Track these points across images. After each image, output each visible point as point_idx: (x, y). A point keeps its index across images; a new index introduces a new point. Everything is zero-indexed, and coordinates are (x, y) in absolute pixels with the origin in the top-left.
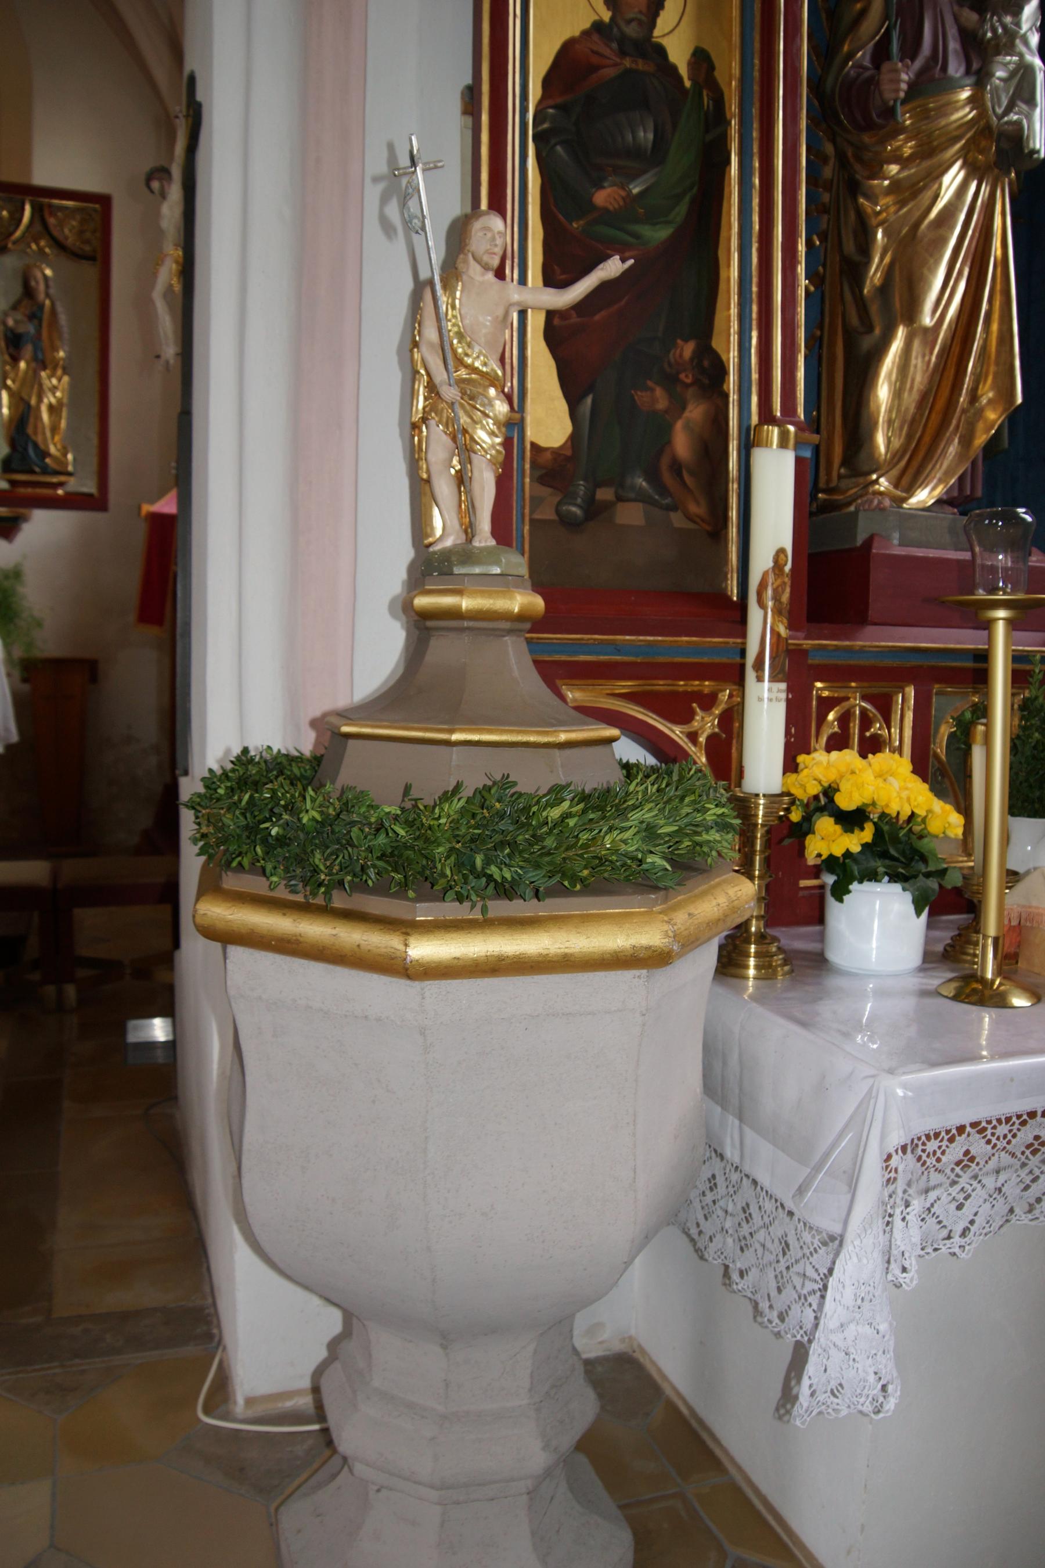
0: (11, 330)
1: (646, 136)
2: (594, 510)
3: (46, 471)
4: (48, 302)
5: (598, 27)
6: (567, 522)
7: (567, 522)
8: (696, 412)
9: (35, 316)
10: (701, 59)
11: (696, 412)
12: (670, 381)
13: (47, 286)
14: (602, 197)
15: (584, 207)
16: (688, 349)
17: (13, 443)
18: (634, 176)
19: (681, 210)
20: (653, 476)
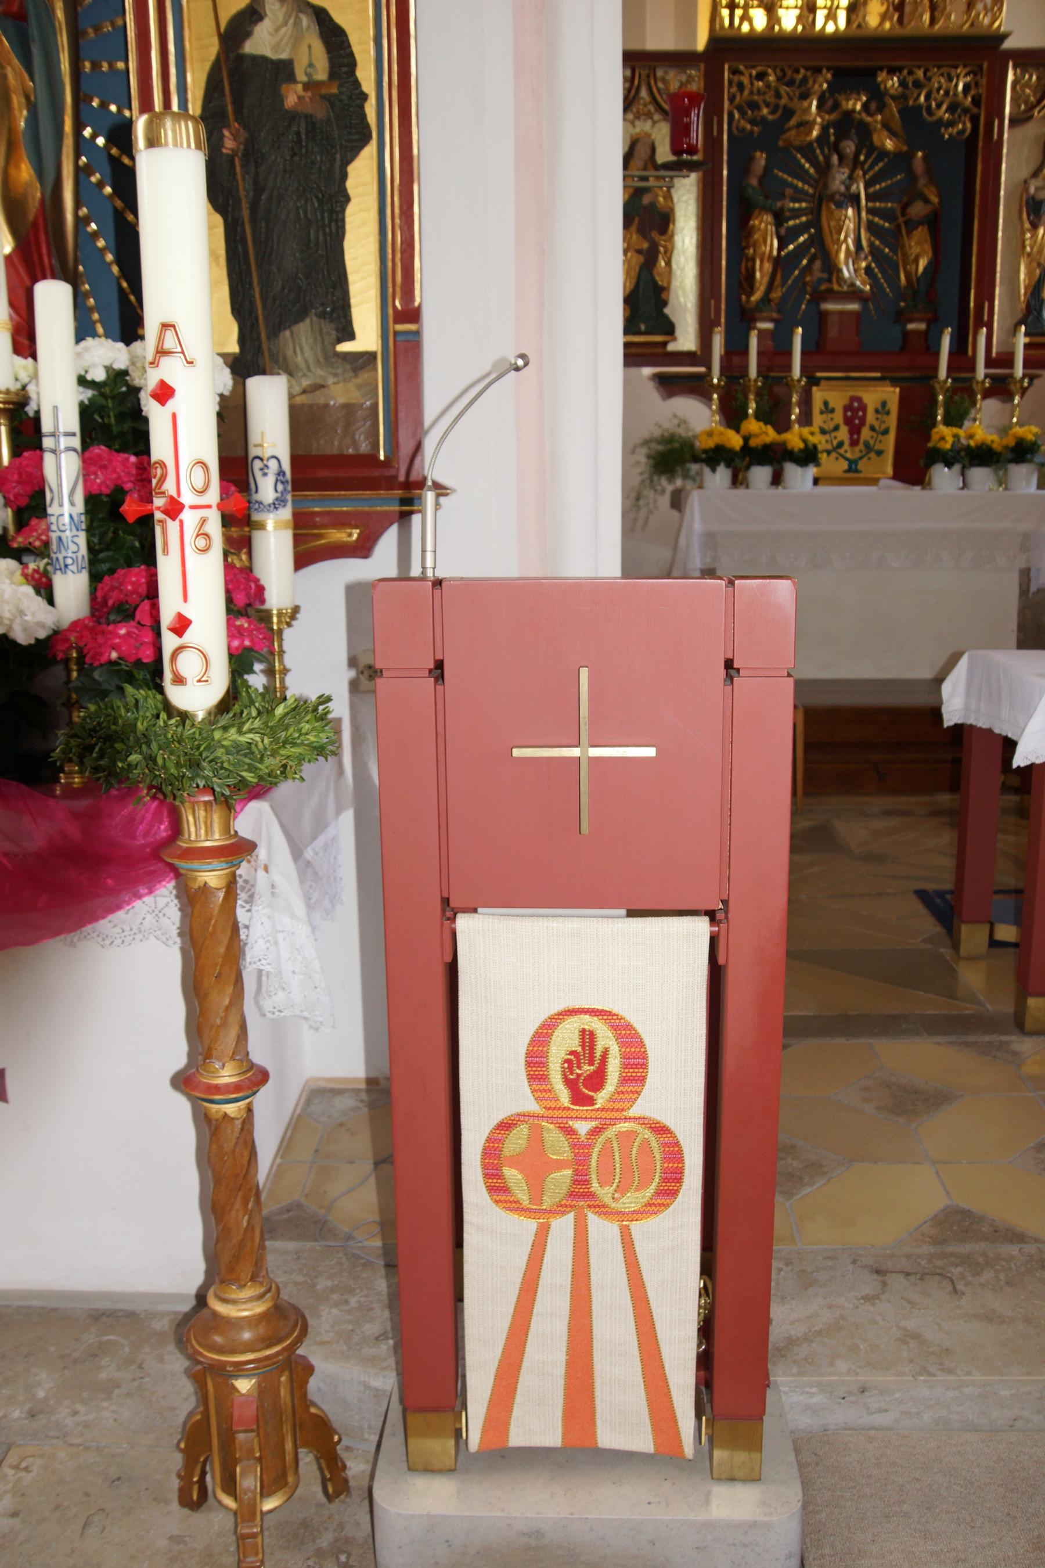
0: (1033, 198)
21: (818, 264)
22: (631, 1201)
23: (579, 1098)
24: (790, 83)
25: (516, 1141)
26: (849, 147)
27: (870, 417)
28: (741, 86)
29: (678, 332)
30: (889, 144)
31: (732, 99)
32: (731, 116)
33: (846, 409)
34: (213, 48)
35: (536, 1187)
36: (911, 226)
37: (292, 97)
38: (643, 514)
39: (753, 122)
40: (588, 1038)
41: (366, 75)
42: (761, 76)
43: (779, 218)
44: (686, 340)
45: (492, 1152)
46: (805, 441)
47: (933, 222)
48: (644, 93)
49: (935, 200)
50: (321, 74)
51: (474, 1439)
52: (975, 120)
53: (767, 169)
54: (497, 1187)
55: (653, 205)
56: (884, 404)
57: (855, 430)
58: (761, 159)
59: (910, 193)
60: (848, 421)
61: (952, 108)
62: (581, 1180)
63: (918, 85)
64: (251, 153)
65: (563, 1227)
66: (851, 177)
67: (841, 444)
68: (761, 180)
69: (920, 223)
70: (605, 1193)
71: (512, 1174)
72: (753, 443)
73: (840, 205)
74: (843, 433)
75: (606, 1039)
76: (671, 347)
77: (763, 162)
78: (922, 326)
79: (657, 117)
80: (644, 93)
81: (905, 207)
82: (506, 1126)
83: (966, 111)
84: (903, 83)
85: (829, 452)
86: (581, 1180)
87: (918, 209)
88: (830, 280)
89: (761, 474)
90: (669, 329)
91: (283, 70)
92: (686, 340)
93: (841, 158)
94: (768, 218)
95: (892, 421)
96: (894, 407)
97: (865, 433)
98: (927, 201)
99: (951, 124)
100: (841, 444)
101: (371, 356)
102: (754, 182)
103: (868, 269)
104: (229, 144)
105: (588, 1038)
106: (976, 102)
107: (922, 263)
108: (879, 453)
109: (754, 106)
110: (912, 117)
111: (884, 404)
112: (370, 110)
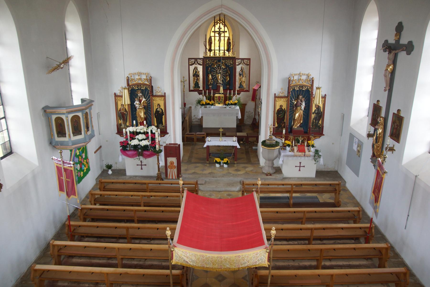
1: (281, 112)
2: (278, 129)
3: (243, 88)
4: (244, 70)
5: (279, 108)
6: (277, 129)
7: (277, 129)
8: (283, 124)
9: (242, 72)
10: (284, 109)
11: (283, 124)
12: (282, 123)
13: (244, 68)
14: (279, 116)
15: (278, 116)
16: (283, 122)
17: (240, 85)
18: (281, 114)
19: (283, 116)
20: (281, 127)
21: (216, 80)
22: (174, 168)
23: (172, 164)
24: (212, 61)
25: (169, 166)
26: (219, 68)
27: (221, 98)
28: (207, 62)
29: (200, 88)
30: (224, 67)
31: (206, 63)
32: (206, 64)
33: (218, 98)
34: (155, 110)
35: (170, 167)
36: (227, 76)
37: (160, 113)
38: (196, 109)
39: (208, 65)
40: (172, 162)
41: (164, 111)
42: (209, 60)
43: (212, 75)
44: (201, 89)
45: (169, 166)
46: (212, 103)
47: (229, 75)
48: (196, 62)
49: (229, 73)
50: (161, 111)
51: (168, 178)
52: (233, 65)
53: (210, 69)
54: (169, 168)
55: (197, 74)
56: (222, 97)
57: (219, 100)
58: (210, 68)
59: (227, 72)
60: (218, 99)
61: (230, 64)
62: (172, 167)
63: (226, 61)
64: (157, 115)
65: (171, 169)
66: (220, 71)
67: (218, 101)
68: (210, 70)
69: (228, 76)
70: (173, 168)
71: (169, 167)
72: (207, 103)
73: (218, 74)
74: (218, 100)
75: (173, 162)
76: (200, 89)
77: (210, 69)
78: (228, 87)
79: (198, 64)
80: (196, 62)
81: (226, 73)
82: (169, 165)
83: (232, 64)
84: (225, 61)
85: (216, 102)
86: (172, 167)
87: (227, 74)
88: (217, 82)
89: (208, 106)
90: (199, 87)
91: (159, 111)
92: (201, 89)
93: (218, 68)
94: (211, 75)
95: (223, 99)
96: (223, 97)
97: (221, 100)
98: (229, 73)
99: (230, 66)
100: (218, 101)
101: (164, 126)
102: (209, 71)
103: (222, 80)
104: (156, 115)
105: (172, 162)
106: (233, 63)
107: (228, 80)
108: (222, 102)
109: (208, 63)
110: (226, 65)
111: (222, 97)
112: (164, 113)
